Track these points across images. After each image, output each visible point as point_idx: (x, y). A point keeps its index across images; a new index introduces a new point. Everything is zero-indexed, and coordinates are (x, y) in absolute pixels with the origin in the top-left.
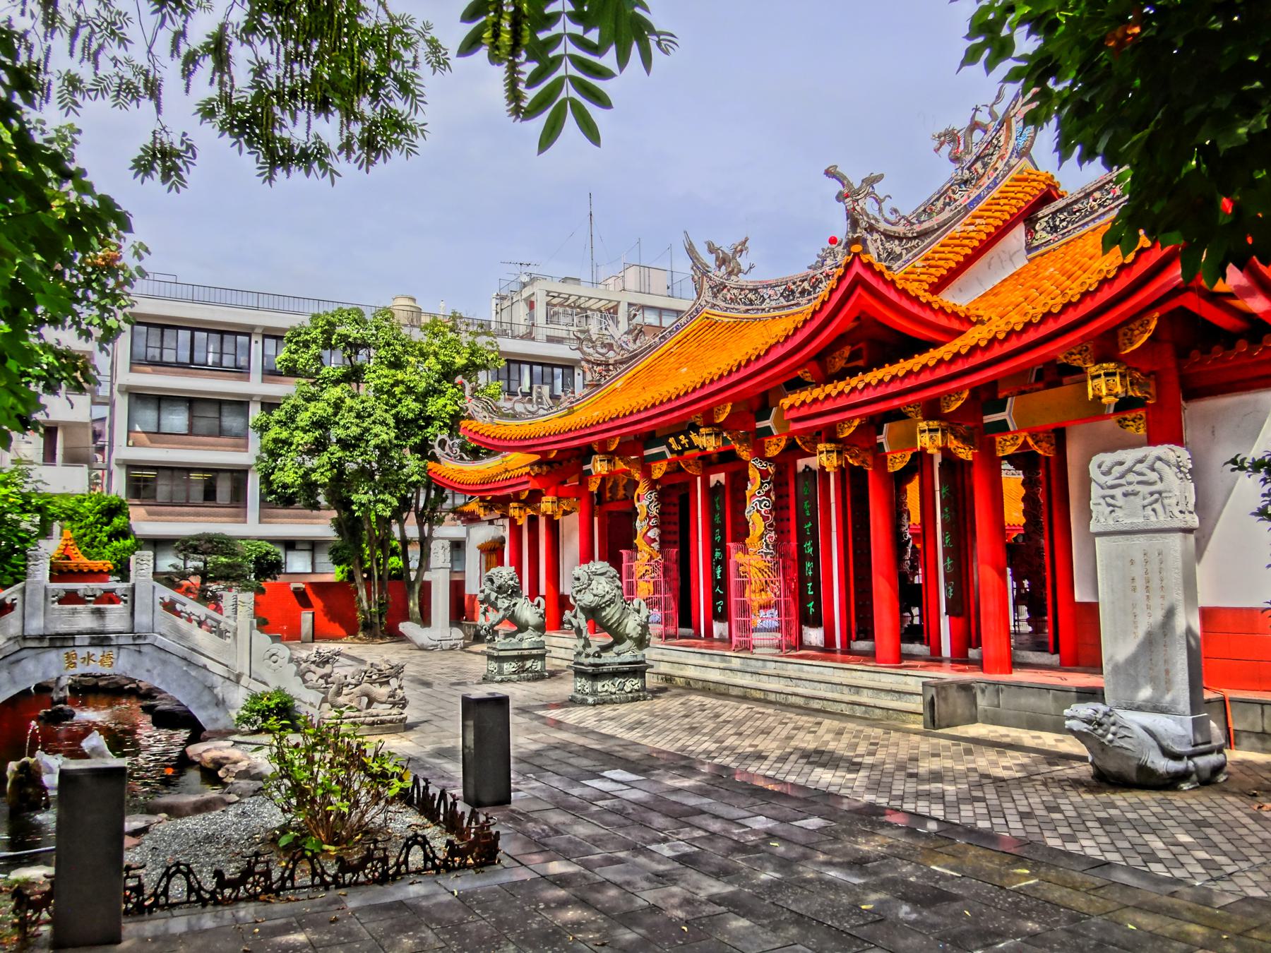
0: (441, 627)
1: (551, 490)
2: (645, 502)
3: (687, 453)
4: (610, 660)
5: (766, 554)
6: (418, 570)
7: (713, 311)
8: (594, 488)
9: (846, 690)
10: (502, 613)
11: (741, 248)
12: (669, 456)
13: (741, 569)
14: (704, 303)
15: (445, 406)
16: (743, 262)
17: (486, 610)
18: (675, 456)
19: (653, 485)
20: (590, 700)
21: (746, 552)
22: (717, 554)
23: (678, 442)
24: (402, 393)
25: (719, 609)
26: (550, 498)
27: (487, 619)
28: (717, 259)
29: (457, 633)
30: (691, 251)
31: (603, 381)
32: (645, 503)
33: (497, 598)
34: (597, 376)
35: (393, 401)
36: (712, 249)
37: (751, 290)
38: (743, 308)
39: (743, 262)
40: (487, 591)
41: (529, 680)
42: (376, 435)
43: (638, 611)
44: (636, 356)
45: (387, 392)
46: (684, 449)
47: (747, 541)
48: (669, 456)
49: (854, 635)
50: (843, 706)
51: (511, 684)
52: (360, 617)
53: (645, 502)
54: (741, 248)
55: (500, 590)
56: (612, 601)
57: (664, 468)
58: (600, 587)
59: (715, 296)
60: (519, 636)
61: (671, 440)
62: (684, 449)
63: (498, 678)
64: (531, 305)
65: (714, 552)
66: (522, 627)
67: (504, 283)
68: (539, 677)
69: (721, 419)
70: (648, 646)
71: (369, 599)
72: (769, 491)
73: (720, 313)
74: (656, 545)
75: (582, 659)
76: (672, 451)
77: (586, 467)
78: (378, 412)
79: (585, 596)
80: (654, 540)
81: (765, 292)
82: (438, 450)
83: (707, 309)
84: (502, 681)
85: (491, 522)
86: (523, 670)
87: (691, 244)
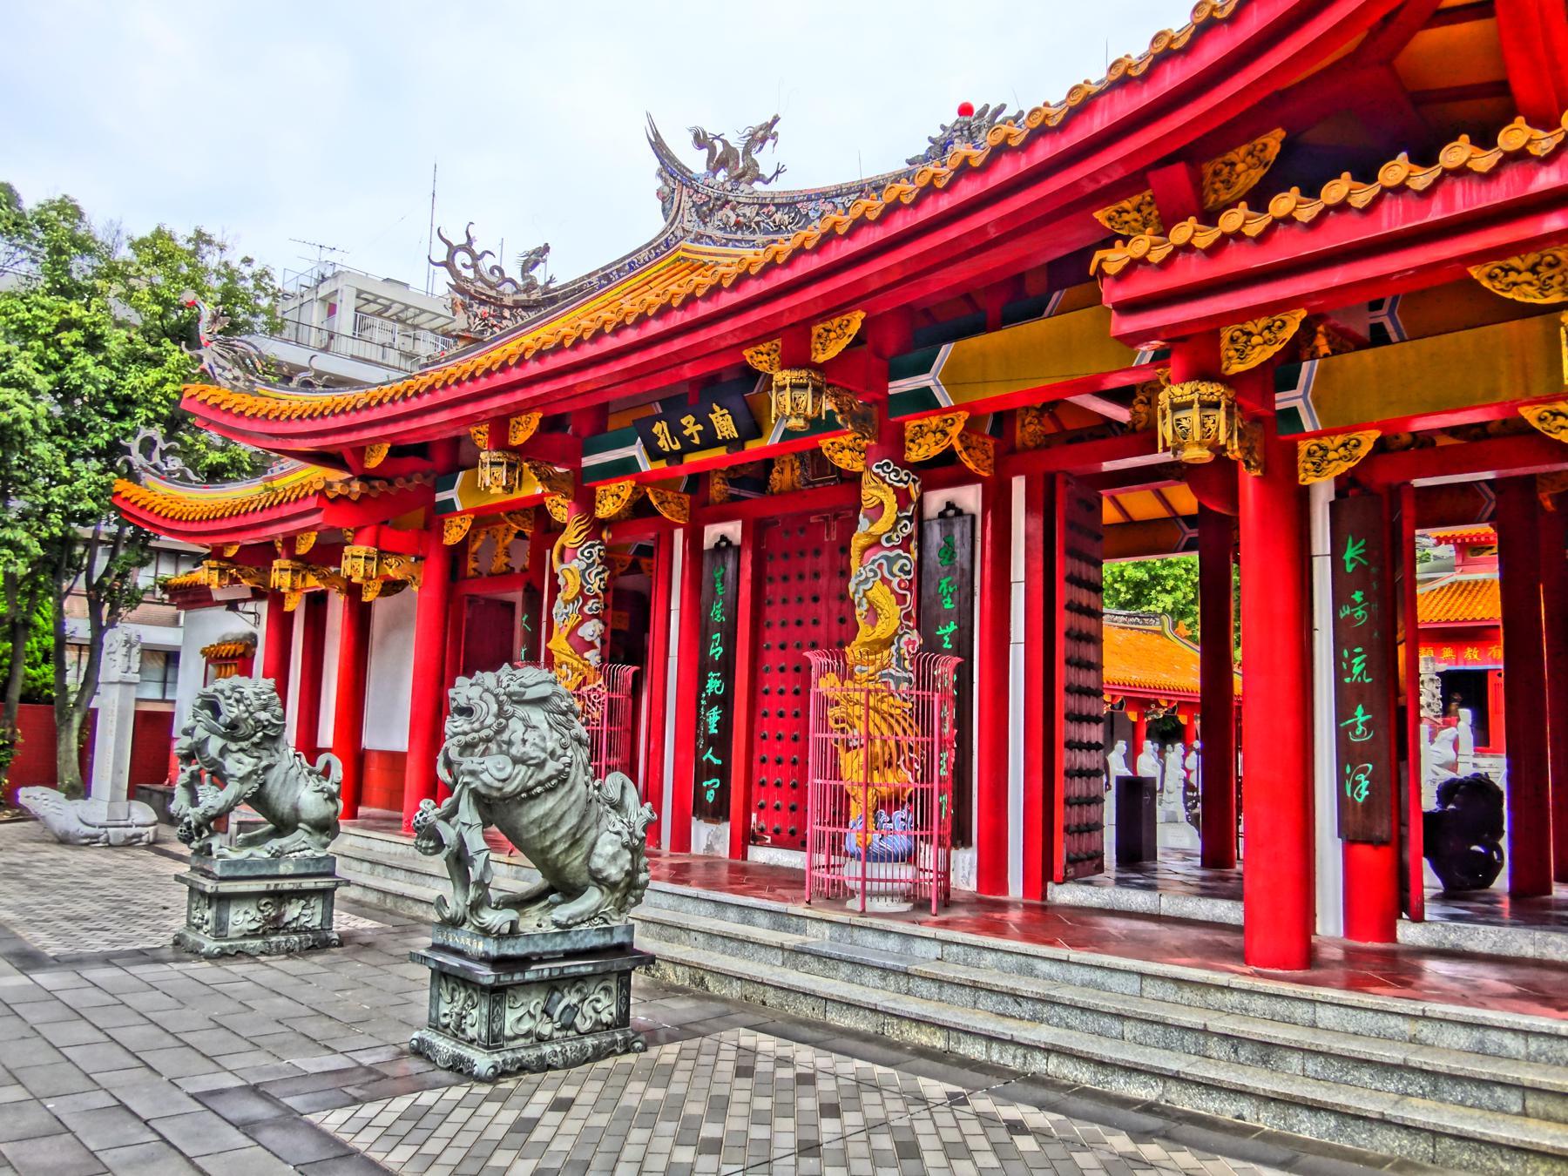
0: (109, 799)
1: (368, 533)
2: (576, 568)
3: (690, 458)
5: (898, 681)
6: (81, 693)
7: (696, 247)
9: (1216, 1048)
10: (233, 789)
11: (764, 134)
12: (646, 466)
13: (833, 712)
14: (679, 233)
15: (162, 382)
16: (766, 159)
17: (196, 778)
18: (662, 464)
19: (596, 527)
20: (483, 1062)
21: (846, 674)
22: (714, 684)
23: (676, 431)
24: (76, 344)
25: (710, 796)
26: (361, 550)
27: (194, 801)
28: (710, 159)
29: (143, 813)
30: (658, 146)
31: (487, 336)
32: (576, 565)
33: (224, 751)
34: (477, 325)
35: (53, 356)
36: (701, 140)
37: (778, 206)
38: (760, 238)
39: (766, 159)
40: (200, 733)
41: (290, 953)
43: (618, 806)
44: (553, 301)
45: (44, 337)
47: (853, 651)
48: (646, 466)
49: (1058, 871)
50: (1246, 1108)
51: (239, 968)
53: (576, 568)
54: (764, 134)
55: (232, 730)
56: (561, 778)
57: (626, 495)
58: (531, 736)
59: (703, 218)
60: (275, 844)
61: (659, 428)
62: (689, 447)
63: (211, 945)
64: (332, 310)
65: (705, 680)
66: (284, 825)
67: (290, 276)
68: (320, 942)
69: (833, 351)
72: (908, 539)
73: (712, 248)
74: (593, 657)
75: (462, 939)
76: (654, 453)
77: (441, 497)
79: (489, 762)
80: (591, 646)
81: (803, 208)
82: (137, 459)
83: (685, 244)
84: (223, 955)
85: (232, 605)
86: (275, 925)
87: (657, 135)
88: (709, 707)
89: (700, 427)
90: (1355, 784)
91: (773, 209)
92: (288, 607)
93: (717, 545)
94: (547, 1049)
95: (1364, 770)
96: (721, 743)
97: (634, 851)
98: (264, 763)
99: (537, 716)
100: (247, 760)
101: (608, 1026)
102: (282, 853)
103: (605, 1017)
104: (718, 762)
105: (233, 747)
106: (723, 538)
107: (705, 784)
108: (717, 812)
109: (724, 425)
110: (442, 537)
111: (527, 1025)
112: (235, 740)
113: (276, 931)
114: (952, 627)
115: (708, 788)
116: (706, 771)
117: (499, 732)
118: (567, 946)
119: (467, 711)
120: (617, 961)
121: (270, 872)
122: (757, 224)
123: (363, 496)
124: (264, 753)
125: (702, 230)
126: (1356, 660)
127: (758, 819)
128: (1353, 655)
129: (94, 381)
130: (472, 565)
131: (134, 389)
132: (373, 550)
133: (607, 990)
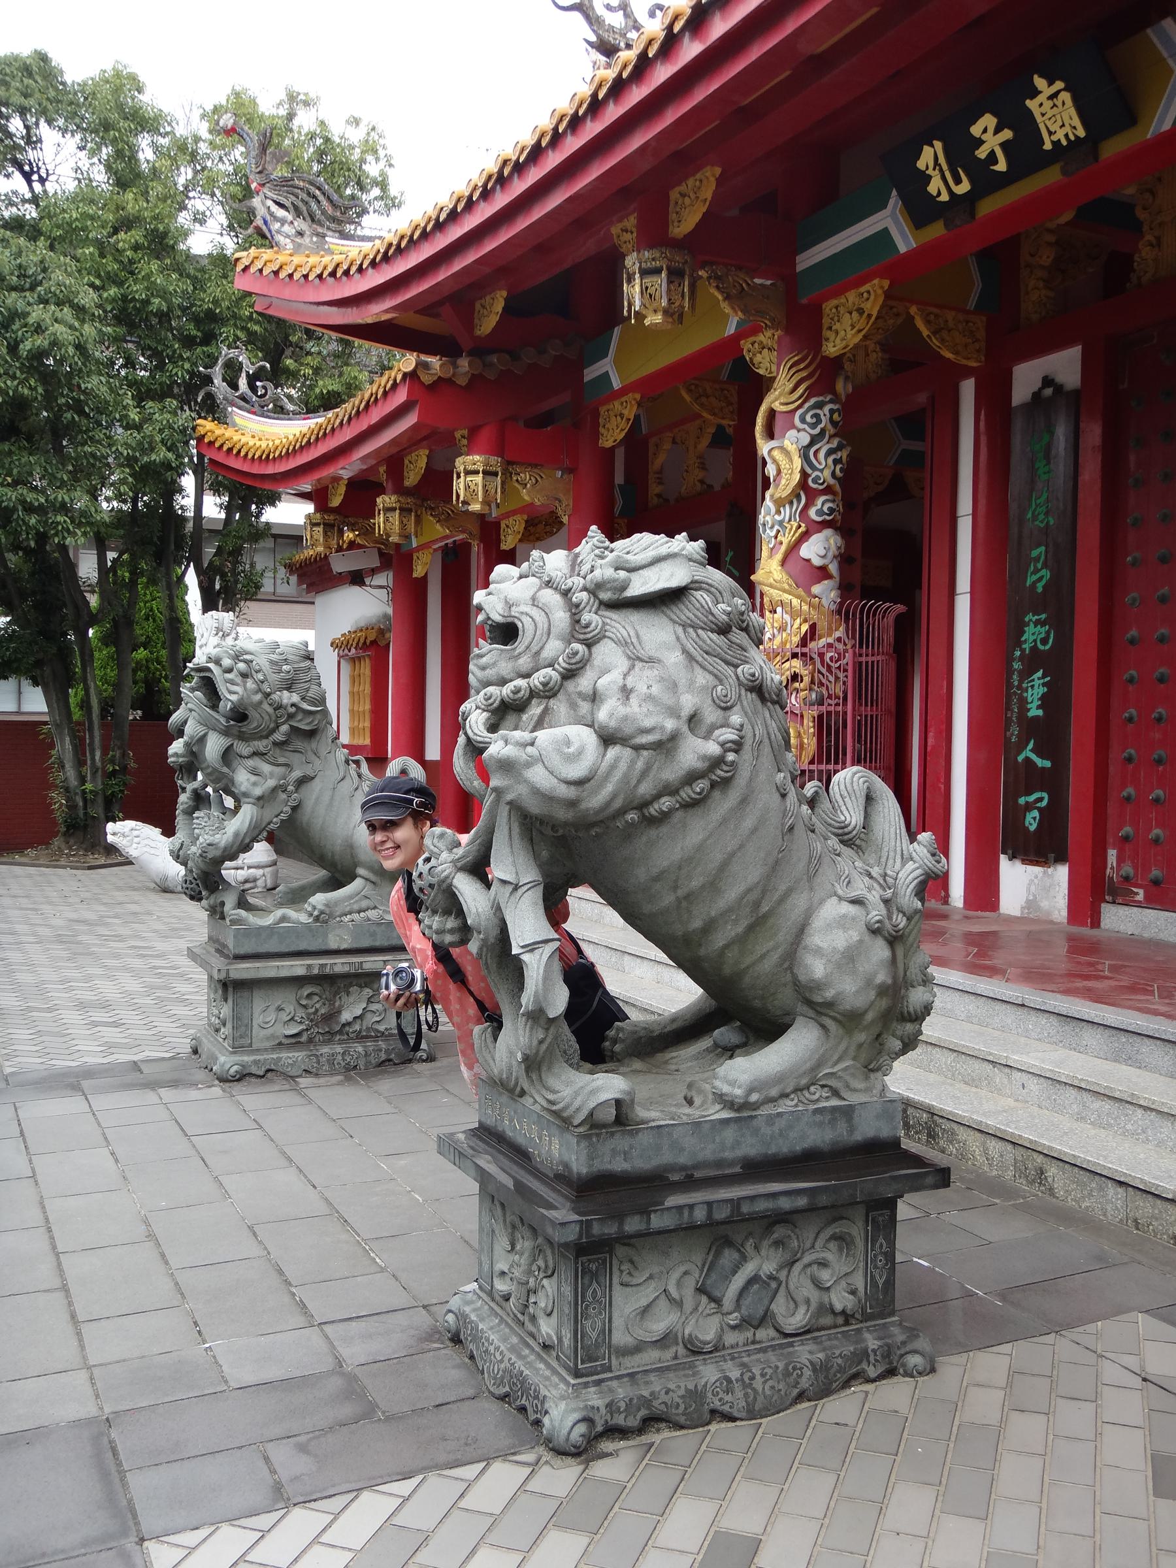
1: (486, 434)
3: (987, 207)
4: (694, 1151)
8: (612, 434)
18: (937, 230)
19: (822, 377)
22: (1033, 634)
23: (961, 153)
24: (136, 247)
26: (476, 460)
33: (227, 755)
42: (39, 329)
46: (986, 180)
52: (58, 801)
56: (716, 775)
57: (873, 307)
58: (644, 681)
70: (910, 1044)
71: (80, 763)
78: (58, 275)
88: (1027, 673)
89: (1007, 134)
92: (418, 572)
93: (1036, 395)
94: (709, 1373)
96: (1049, 732)
97: (894, 940)
98: (297, 774)
99: (656, 633)
100: (266, 768)
101: (847, 1317)
102: (331, 916)
103: (840, 1300)
104: (1041, 763)
105: (243, 748)
106: (1047, 381)
107: (1022, 801)
109: (1056, 115)
111: (659, 1325)
112: (242, 737)
113: (329, 1038)
115: (1029, 807)
116: (1030, 778)
117: (570, 674)
118: (751, 1147)
119: (507, 633)
120: (870, 1174)
121: (314, 946)
123: (474, 379)
124: (295, 759)
127: (1120, 860)
129: (164, 294)
130: (655, 489)
131: (216, 302)
132: (495, 461)
133: (843, 1240)
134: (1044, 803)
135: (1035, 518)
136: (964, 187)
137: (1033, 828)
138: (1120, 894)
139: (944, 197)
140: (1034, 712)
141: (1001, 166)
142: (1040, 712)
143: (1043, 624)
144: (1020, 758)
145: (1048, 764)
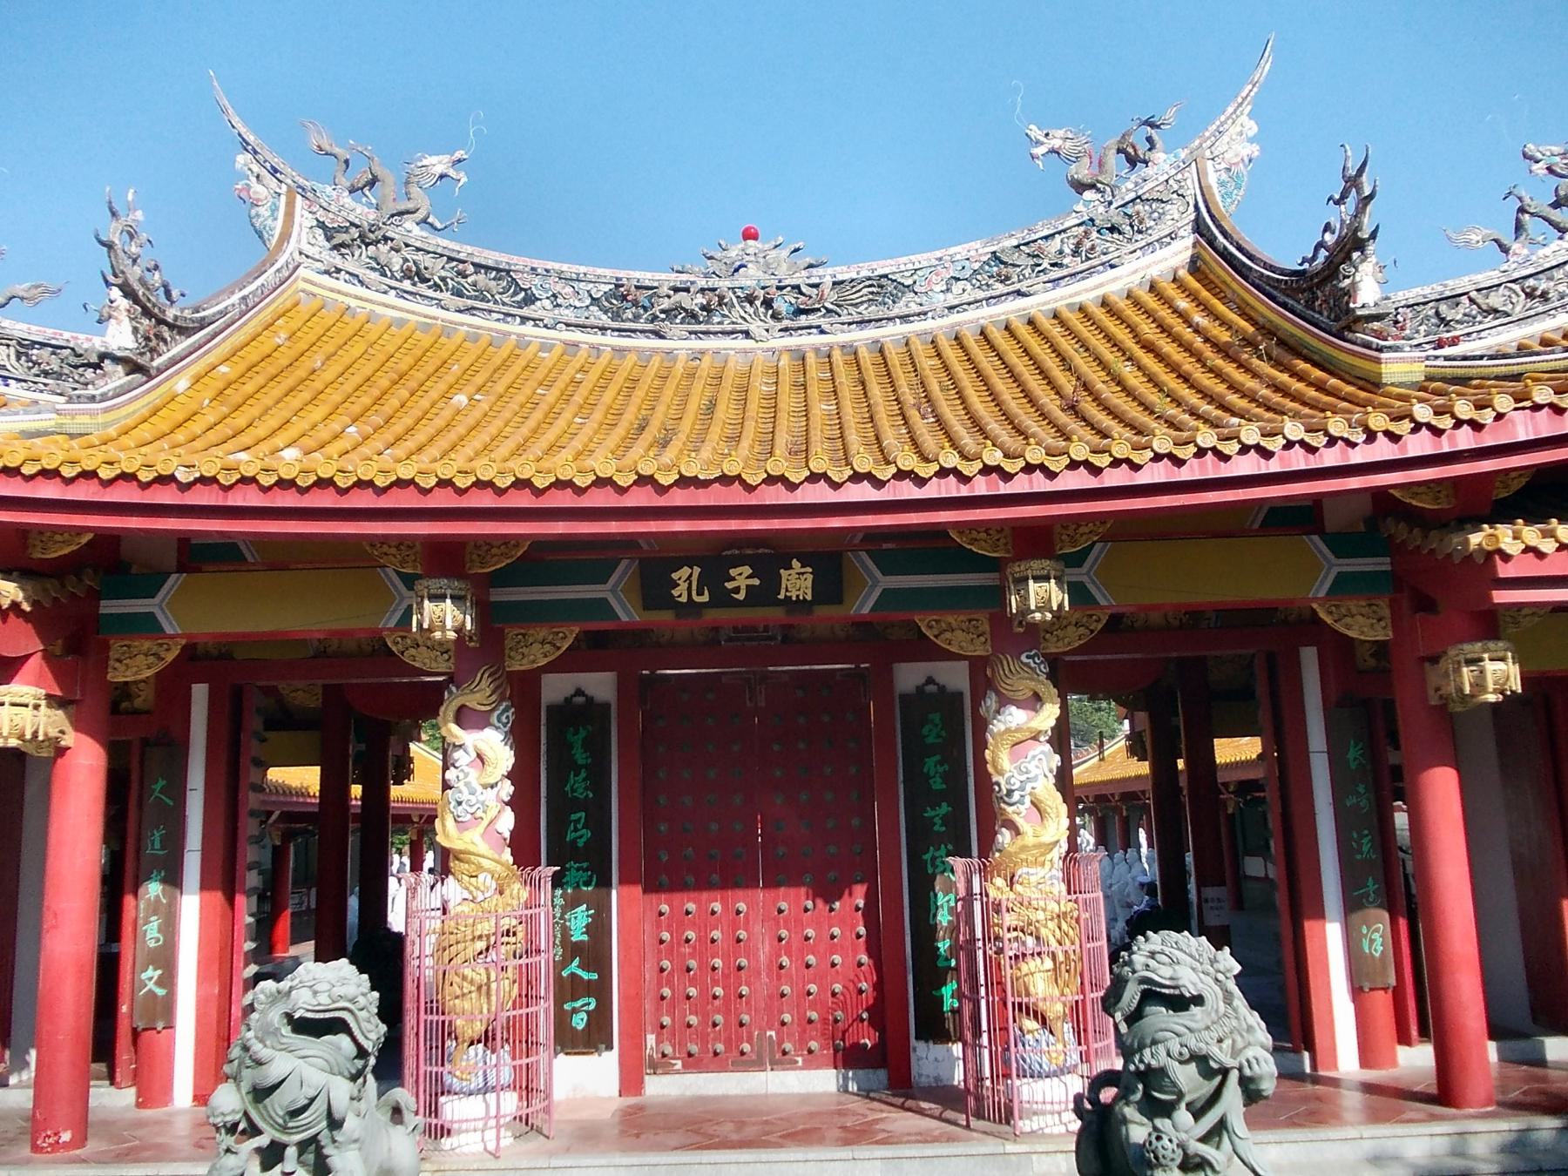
89: (756, 582)
90: (1372, 941)
91: (471, 269)
95: (1377, 930)
104: (585, 975)
108: (593, 1038)
110: (103, 666)
114: (945, 808)
122: (443, 279)
125: (338, 261)
126: (1365, 841)
127: (658, 1042)
128: (1361, 837)
134: (592, 1007)
135: (573, 791)
136: (705, 598)
137: (581, 1026)
138: (660, 1065)
139: (684, 599)
140: (578, 936)
141: (741, 596)
142: (585, 938)
143: (586, 870)
144: (565, 974)
145: (595, 976)
